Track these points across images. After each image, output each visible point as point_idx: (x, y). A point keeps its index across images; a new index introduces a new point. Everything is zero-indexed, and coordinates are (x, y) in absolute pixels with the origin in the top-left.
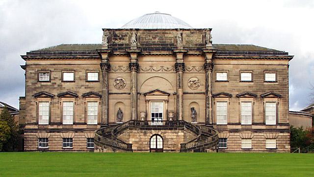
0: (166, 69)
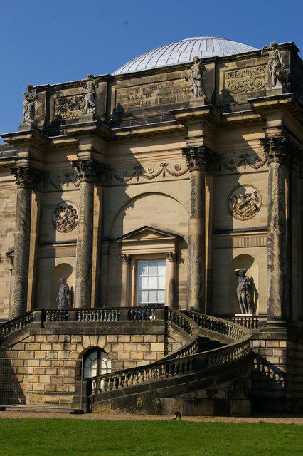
0: (172, 169)
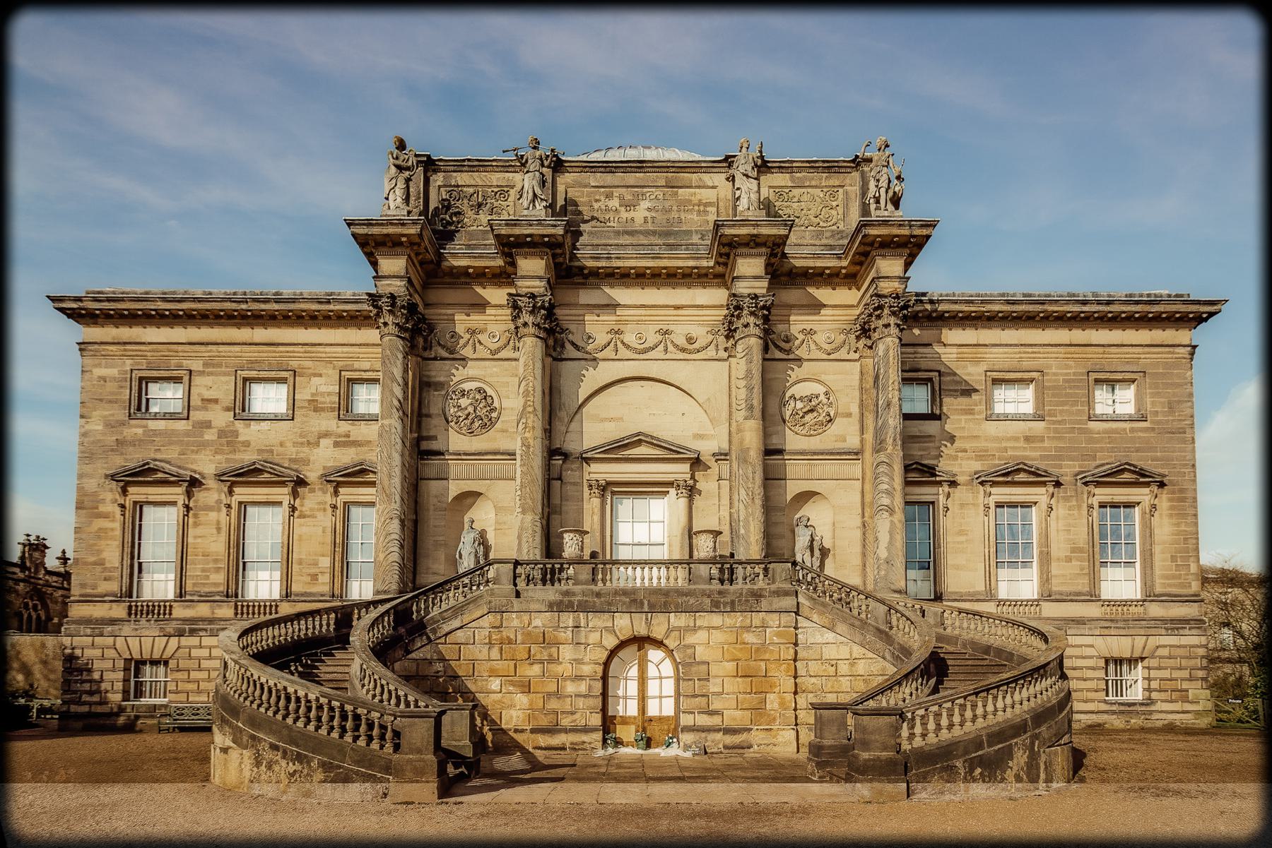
0: (681, 341)
